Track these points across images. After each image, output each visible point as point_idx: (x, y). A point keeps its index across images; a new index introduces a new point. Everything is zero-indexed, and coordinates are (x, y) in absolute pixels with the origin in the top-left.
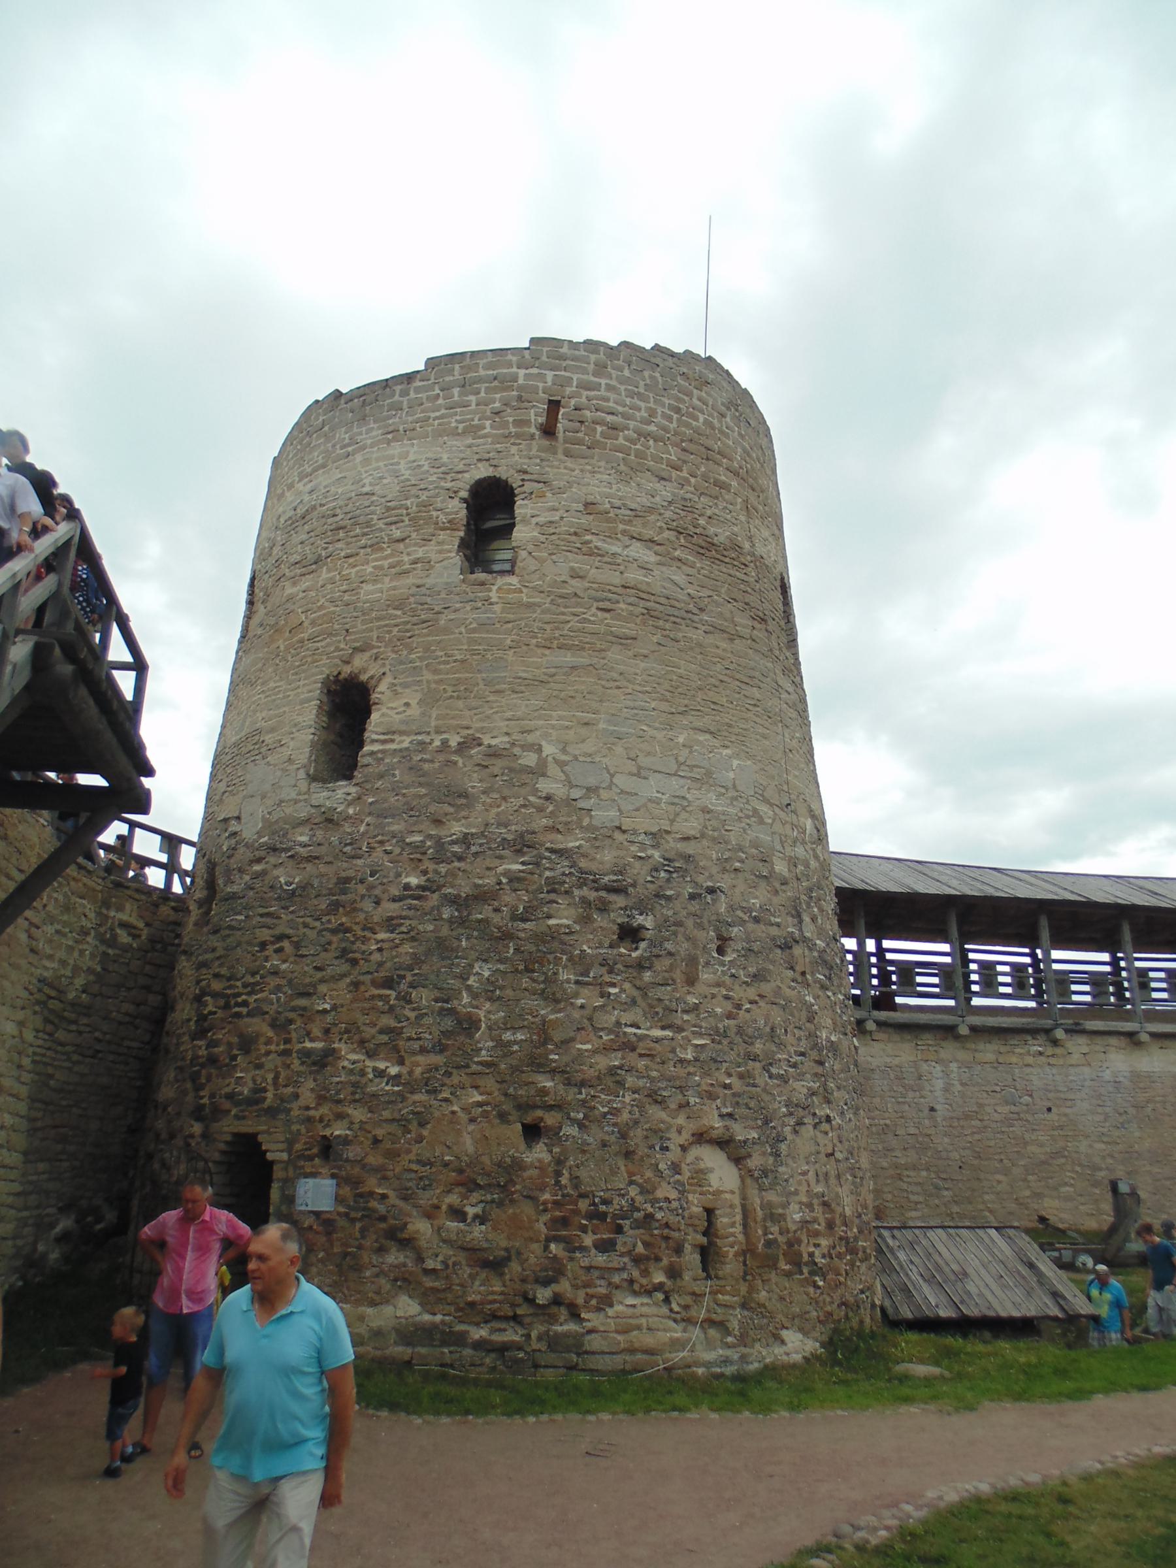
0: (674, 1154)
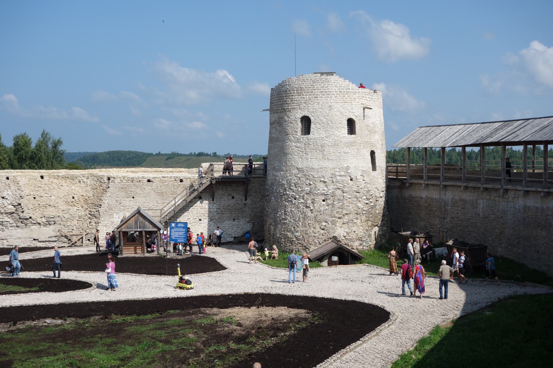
0: (268, 226)
